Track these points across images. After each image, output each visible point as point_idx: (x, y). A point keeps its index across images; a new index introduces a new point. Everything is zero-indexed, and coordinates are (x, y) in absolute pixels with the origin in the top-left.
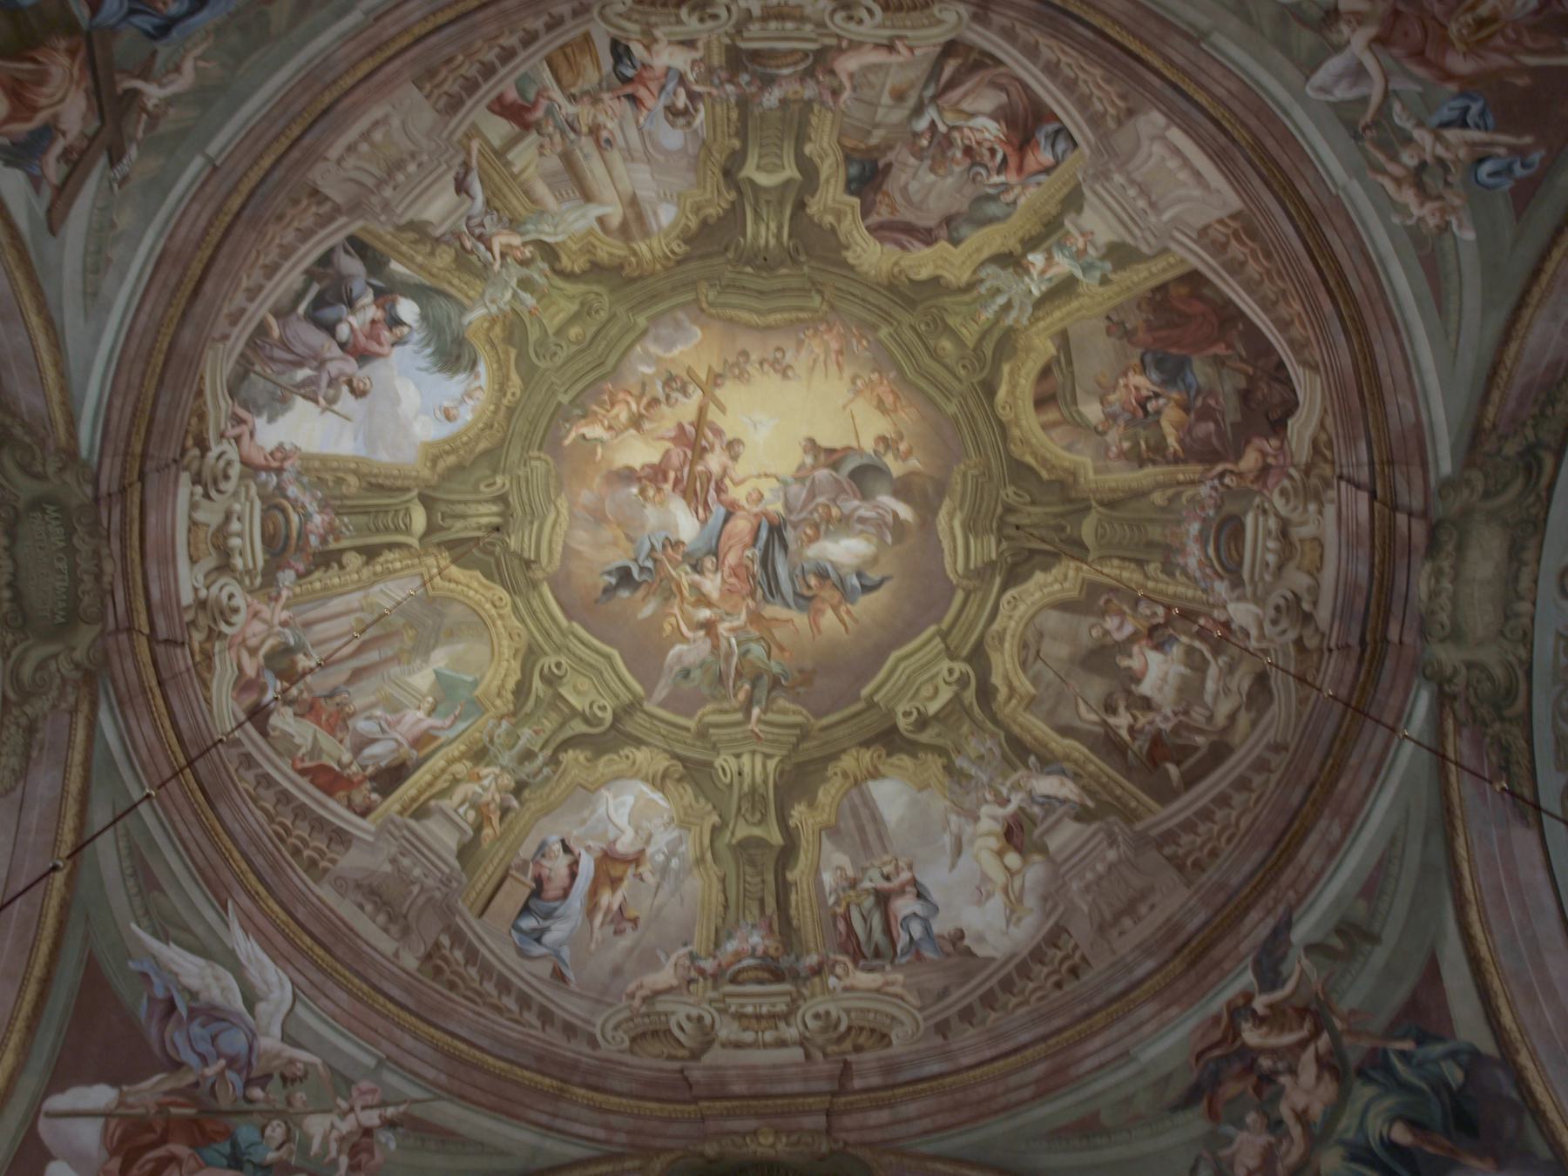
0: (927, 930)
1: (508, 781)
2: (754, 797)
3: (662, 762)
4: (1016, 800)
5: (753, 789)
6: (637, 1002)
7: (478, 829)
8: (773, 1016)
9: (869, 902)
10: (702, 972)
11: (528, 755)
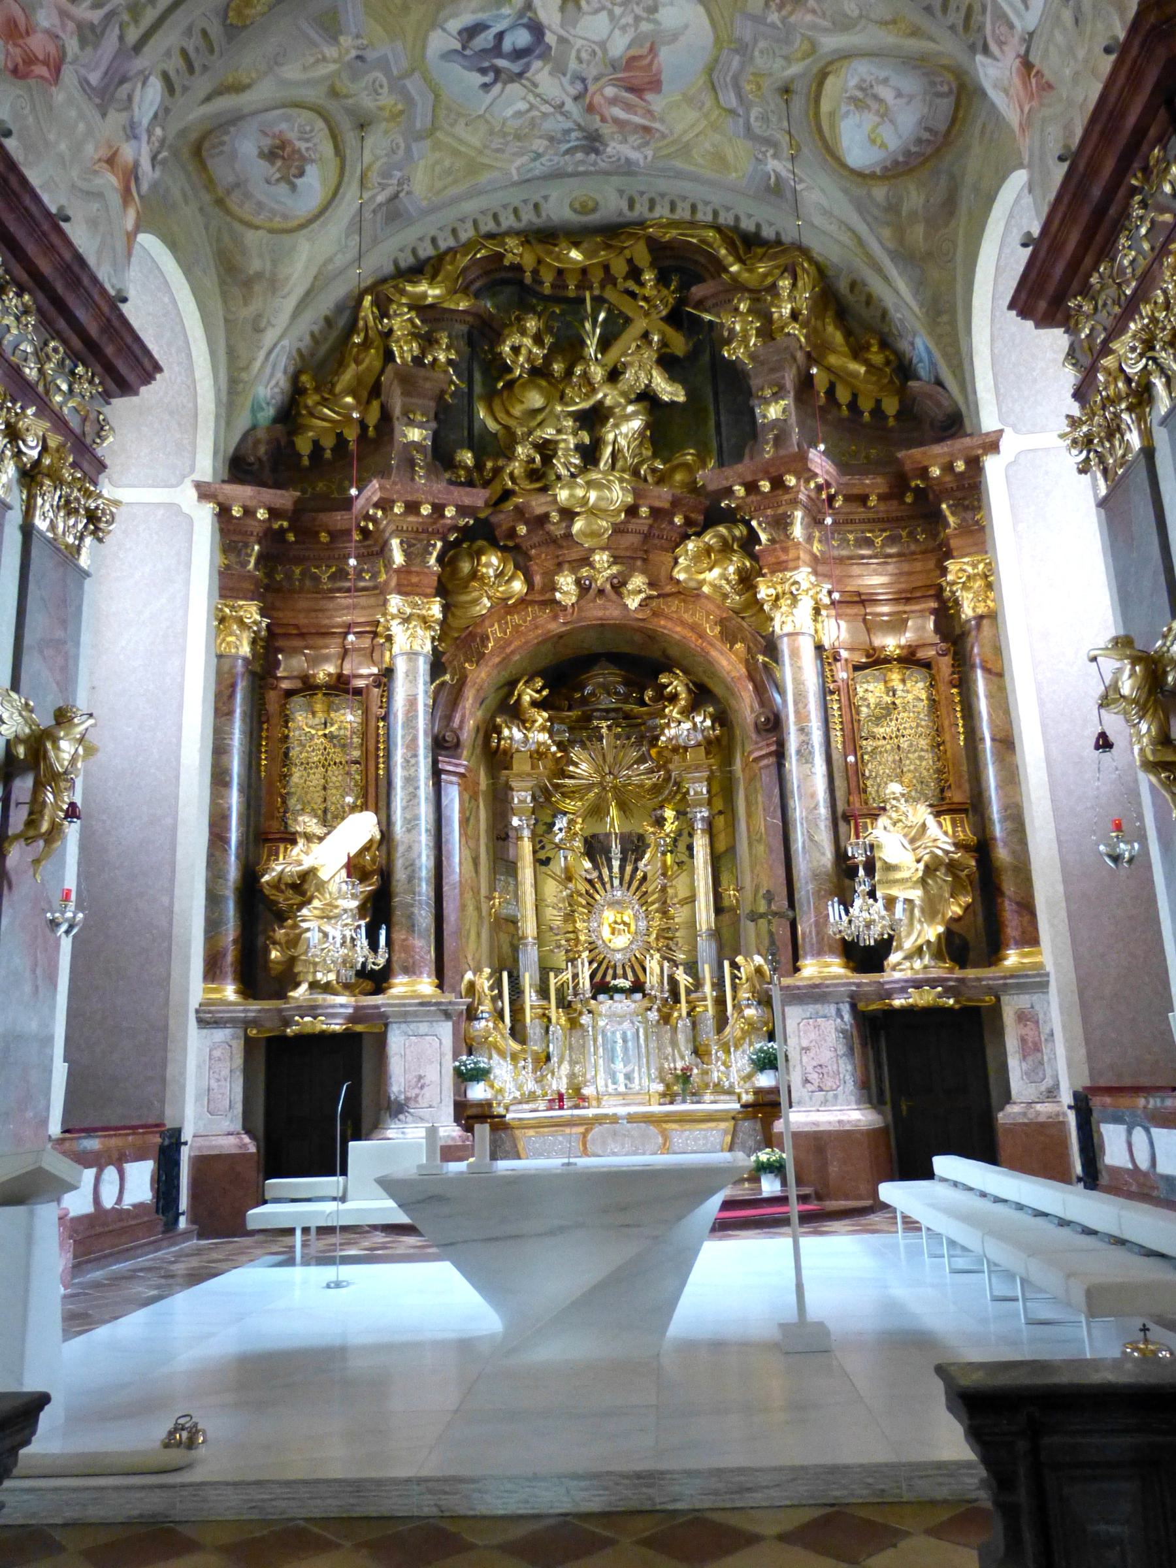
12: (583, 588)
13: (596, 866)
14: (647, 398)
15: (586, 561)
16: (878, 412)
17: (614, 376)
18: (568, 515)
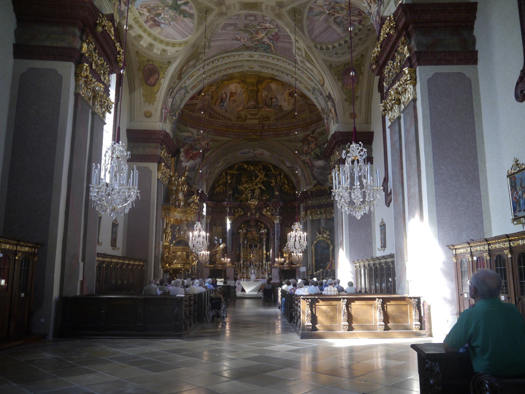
0: (277, 104)
1: (216, 87)
2: (253, 84)
3: (239, 81)
4: (291, 90)
5: (252, 83)
6: (237, 113)
7: (213, 94)
8: (255, 114)
9: (269, 99)
10: (245, 107)
11: (218, 83)
12: (251, 214)
13: (251, 248)
14: (261, 187)
15: (252, 210)
16: (290, 193)
17: (256, 184)
18: (250, 205)
